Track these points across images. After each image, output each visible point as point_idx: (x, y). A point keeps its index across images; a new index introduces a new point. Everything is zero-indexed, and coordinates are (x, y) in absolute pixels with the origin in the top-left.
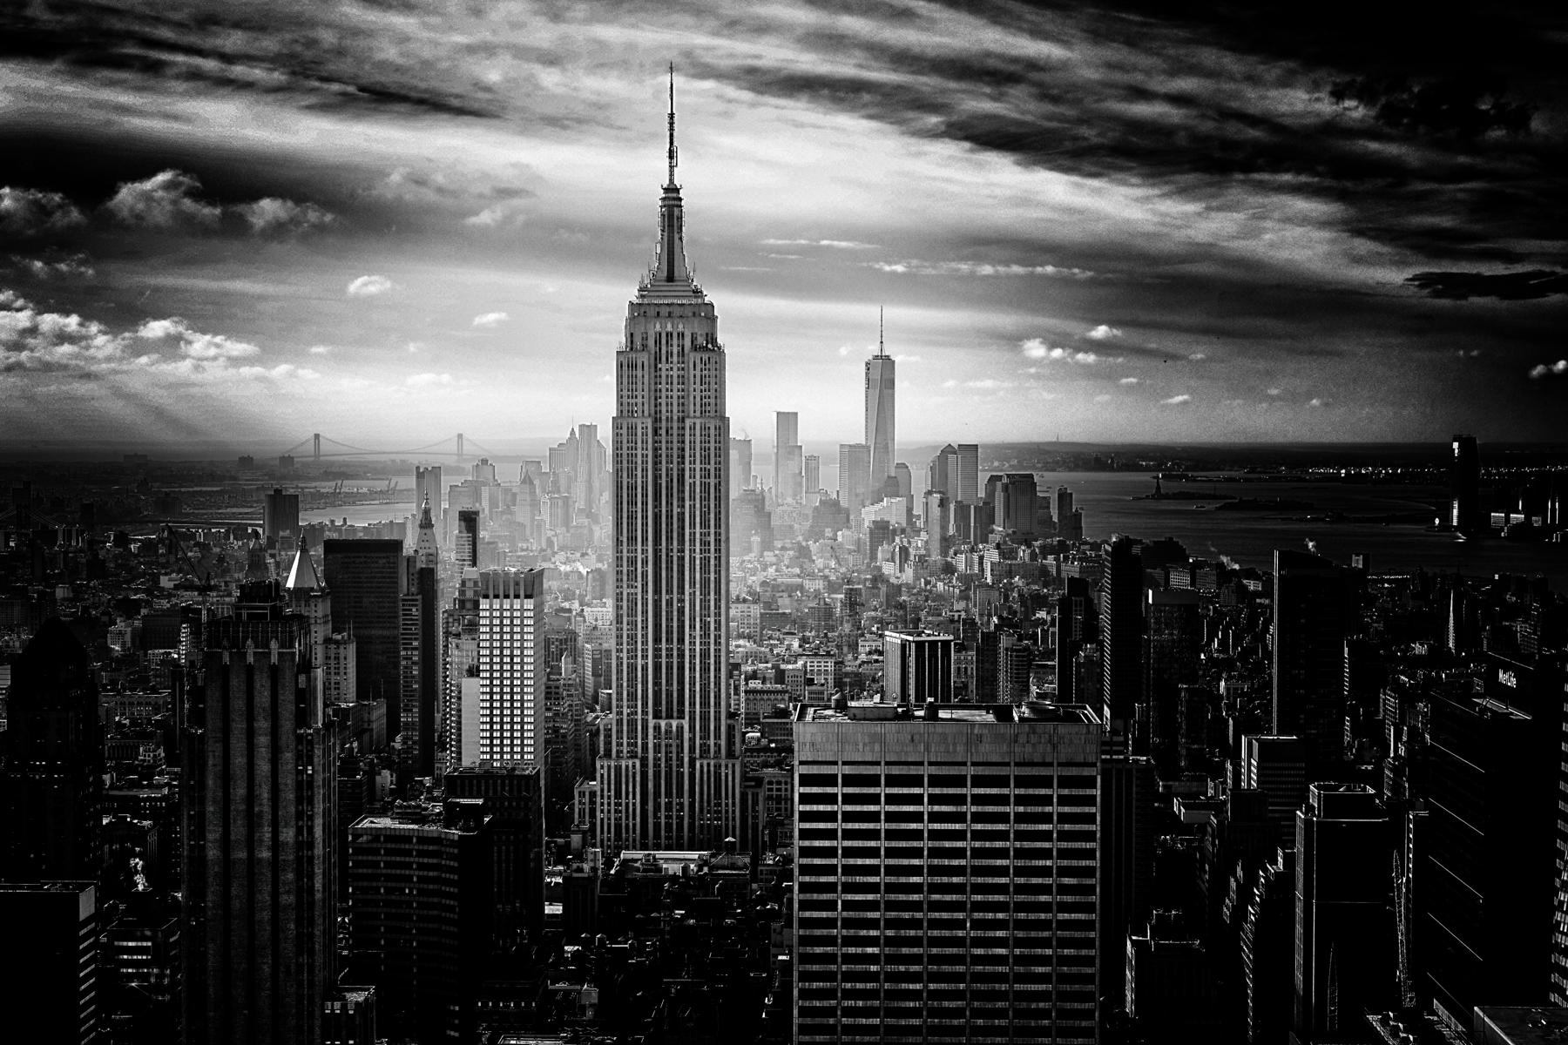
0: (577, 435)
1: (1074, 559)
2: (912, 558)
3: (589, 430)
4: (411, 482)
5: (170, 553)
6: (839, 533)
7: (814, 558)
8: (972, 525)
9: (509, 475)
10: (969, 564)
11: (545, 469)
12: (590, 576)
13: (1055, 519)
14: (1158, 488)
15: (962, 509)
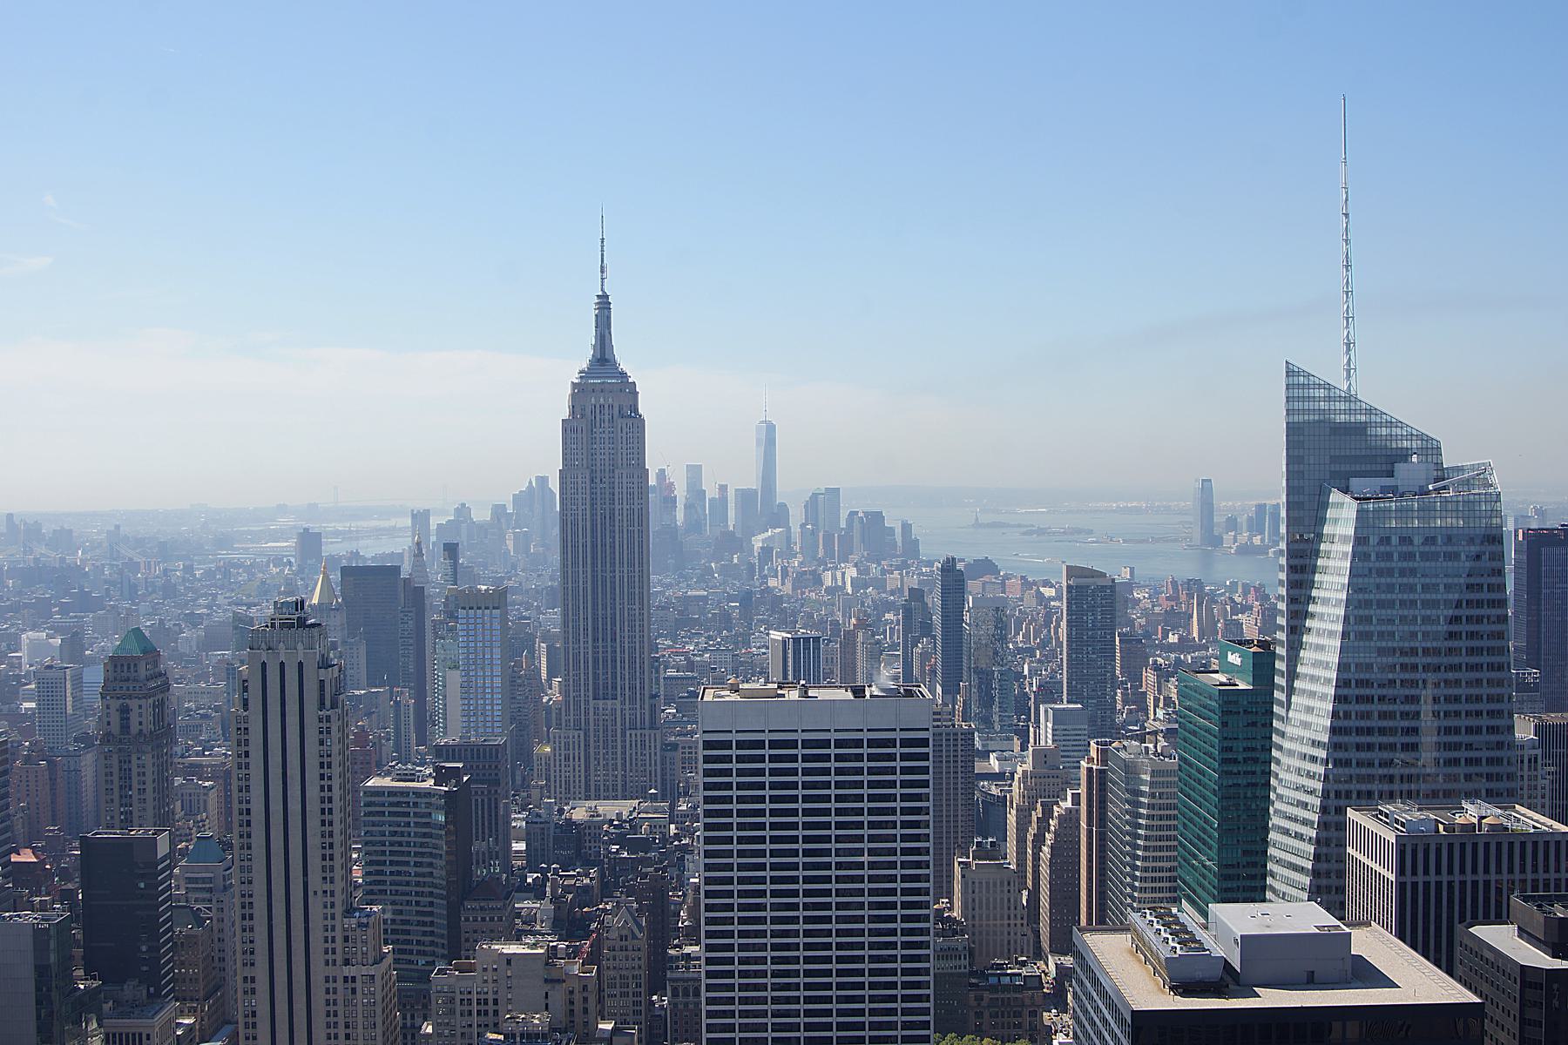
0: (534, 485)
1: (913, 574)
2: (790, 574)
3: (543, 481)
4: (409, 522)
5: (225, 577)
6: (736, 556)
7: (716, 575)
8: (836, 549)
9: (481, 515)
10: (834, 578)
11: (510, 511)
12: (544, 592)
13: (899, 543)
14: (977, 519)
15: (828, 539)
